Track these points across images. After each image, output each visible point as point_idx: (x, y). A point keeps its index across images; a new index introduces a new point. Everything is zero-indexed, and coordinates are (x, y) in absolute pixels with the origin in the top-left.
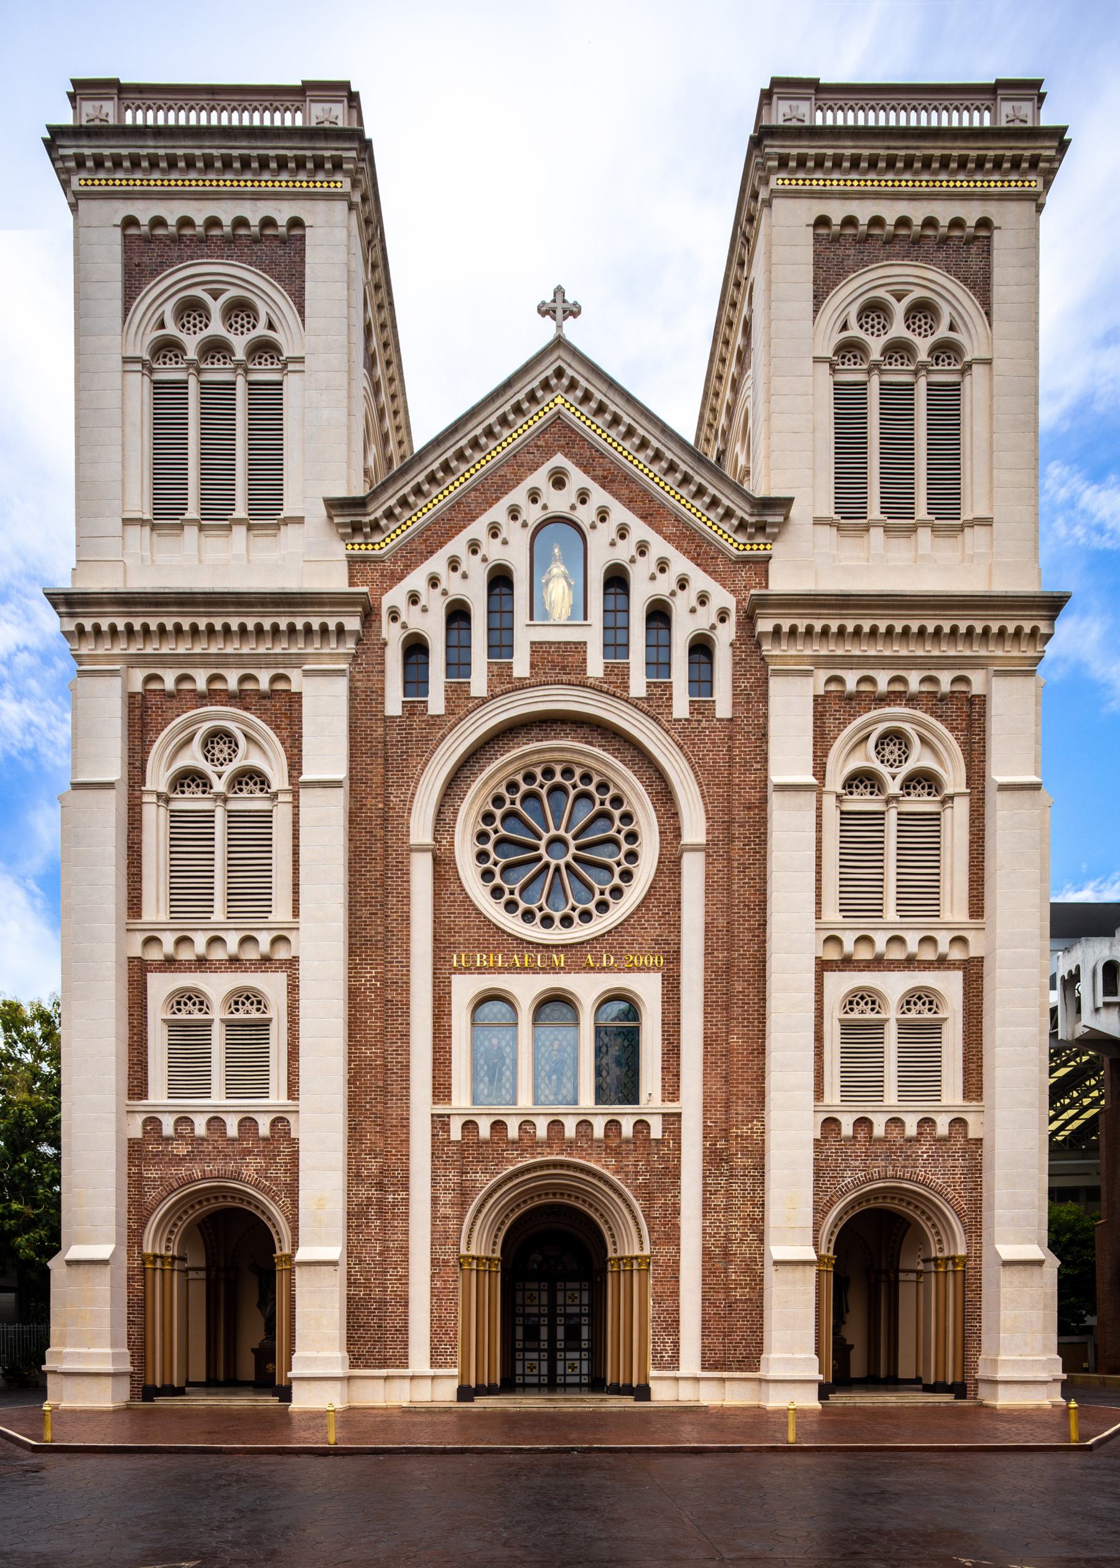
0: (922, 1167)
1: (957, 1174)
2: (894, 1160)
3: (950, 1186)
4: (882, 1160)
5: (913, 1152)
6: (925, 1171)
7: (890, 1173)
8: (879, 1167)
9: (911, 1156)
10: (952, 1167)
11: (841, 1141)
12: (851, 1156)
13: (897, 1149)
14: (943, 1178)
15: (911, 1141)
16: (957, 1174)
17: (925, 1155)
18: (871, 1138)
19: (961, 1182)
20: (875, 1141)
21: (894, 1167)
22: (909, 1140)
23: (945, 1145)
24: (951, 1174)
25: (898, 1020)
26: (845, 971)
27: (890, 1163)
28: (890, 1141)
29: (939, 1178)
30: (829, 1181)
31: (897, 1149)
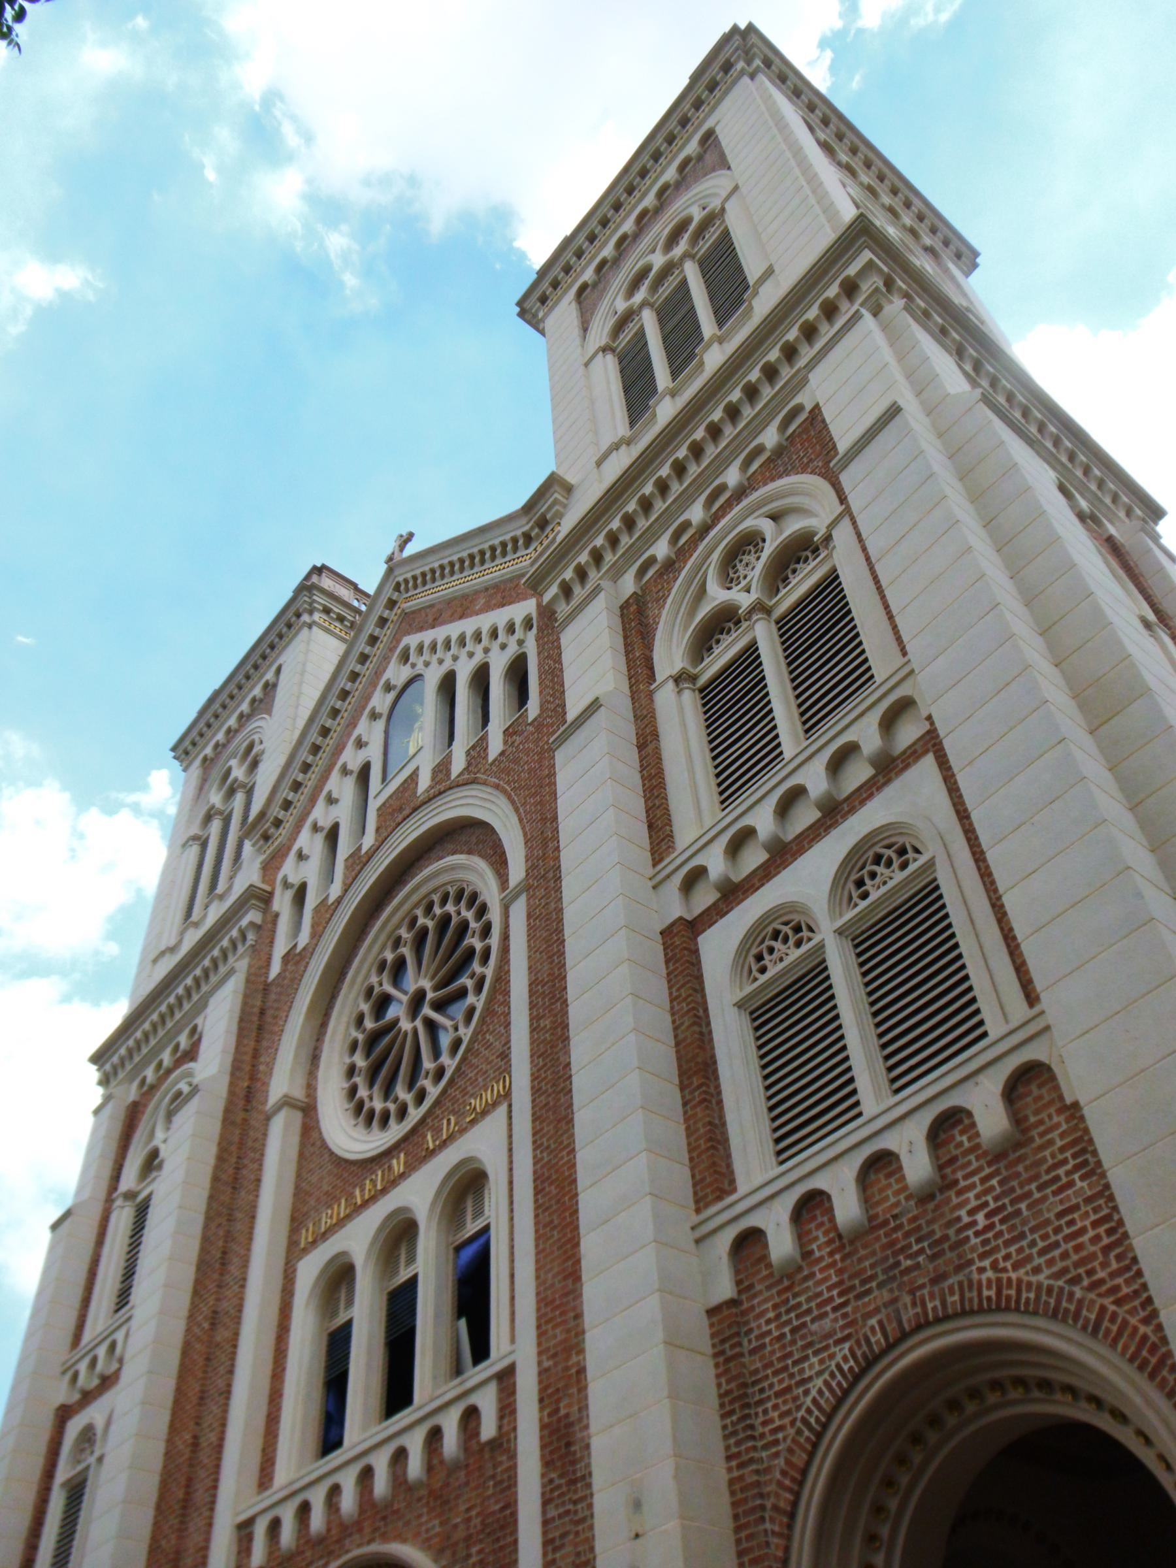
0: (982, 1257)
1: (1082, 1231)
2: (908, 1270)
3: (1075, 1280)
4: (880, 1286)
5: (949, 1224)
6: (994, 1266)
7: (909, 1315)
8: (877, 1310)
9: (946, 1238)
10: (1060, 1215)
11: (780, 1281)
12: (809, 1311)
13: (907, 1235)
14: (1051, 1263)
15: (932, 1197)
16: (1082, 1231)
17: (980, 1217)
18: (840, 1236)
19: (1106, 1250)
20: (852, 1242)
21: (912, 1292)
22: (926, 1197)
23: (1020, 1160)
24: (1067, 1238)
25: (840, 932)
26: (732, 909)
27: (900, 1287)
28: (886, 1223)
29: (1037, 1270)
30: (776, 1407)
31: (907, 1235)
